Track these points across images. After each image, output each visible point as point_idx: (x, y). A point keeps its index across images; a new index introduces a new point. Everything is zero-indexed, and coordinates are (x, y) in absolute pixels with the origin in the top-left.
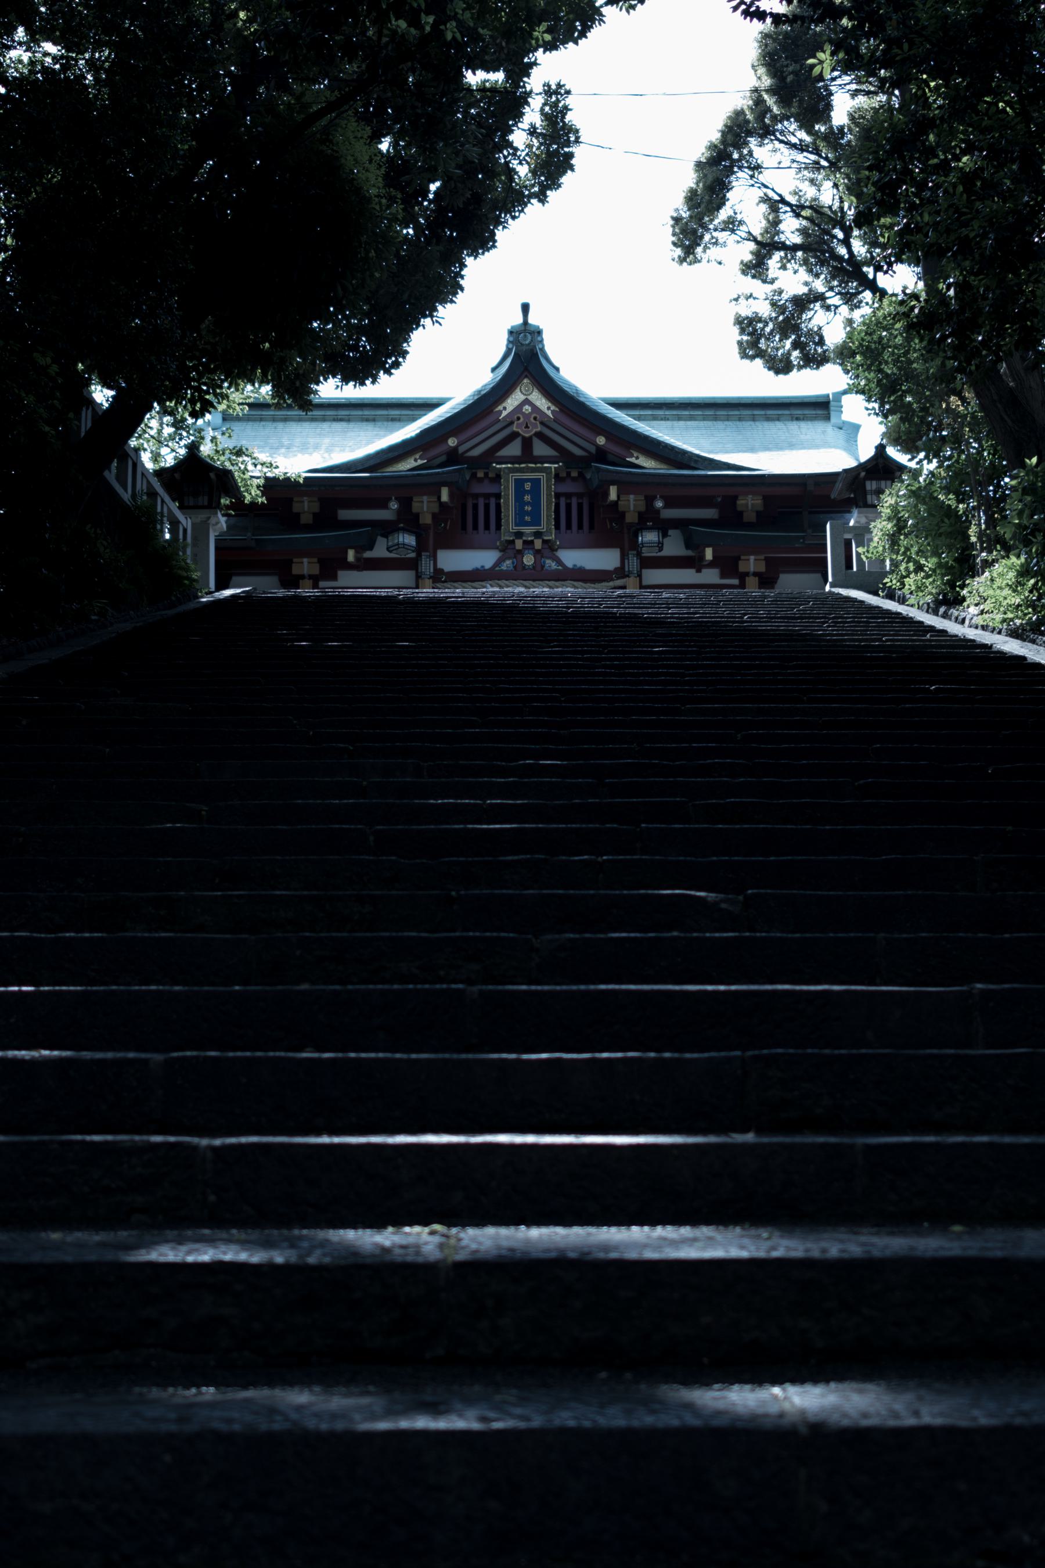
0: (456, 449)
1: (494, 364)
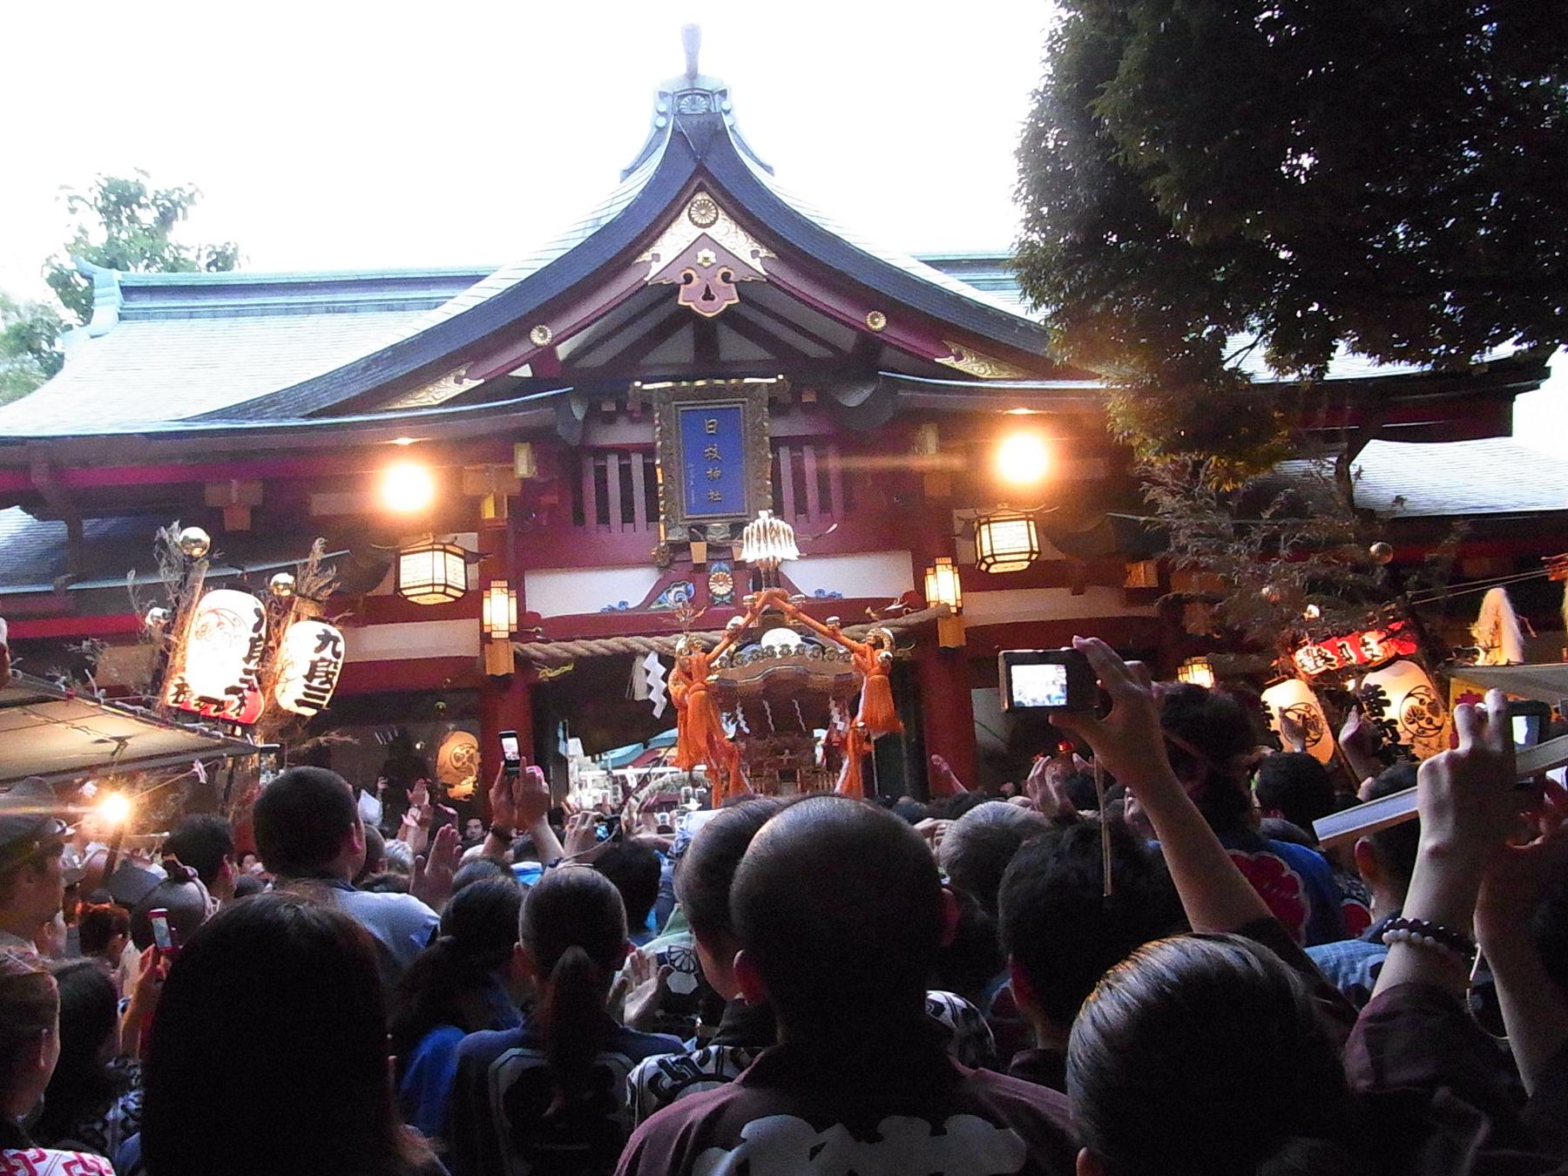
0: (550, 350)
1: (627, 165)
